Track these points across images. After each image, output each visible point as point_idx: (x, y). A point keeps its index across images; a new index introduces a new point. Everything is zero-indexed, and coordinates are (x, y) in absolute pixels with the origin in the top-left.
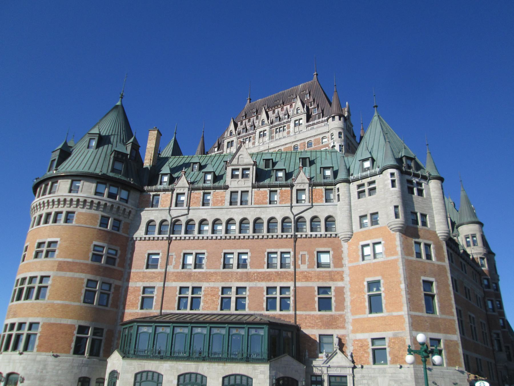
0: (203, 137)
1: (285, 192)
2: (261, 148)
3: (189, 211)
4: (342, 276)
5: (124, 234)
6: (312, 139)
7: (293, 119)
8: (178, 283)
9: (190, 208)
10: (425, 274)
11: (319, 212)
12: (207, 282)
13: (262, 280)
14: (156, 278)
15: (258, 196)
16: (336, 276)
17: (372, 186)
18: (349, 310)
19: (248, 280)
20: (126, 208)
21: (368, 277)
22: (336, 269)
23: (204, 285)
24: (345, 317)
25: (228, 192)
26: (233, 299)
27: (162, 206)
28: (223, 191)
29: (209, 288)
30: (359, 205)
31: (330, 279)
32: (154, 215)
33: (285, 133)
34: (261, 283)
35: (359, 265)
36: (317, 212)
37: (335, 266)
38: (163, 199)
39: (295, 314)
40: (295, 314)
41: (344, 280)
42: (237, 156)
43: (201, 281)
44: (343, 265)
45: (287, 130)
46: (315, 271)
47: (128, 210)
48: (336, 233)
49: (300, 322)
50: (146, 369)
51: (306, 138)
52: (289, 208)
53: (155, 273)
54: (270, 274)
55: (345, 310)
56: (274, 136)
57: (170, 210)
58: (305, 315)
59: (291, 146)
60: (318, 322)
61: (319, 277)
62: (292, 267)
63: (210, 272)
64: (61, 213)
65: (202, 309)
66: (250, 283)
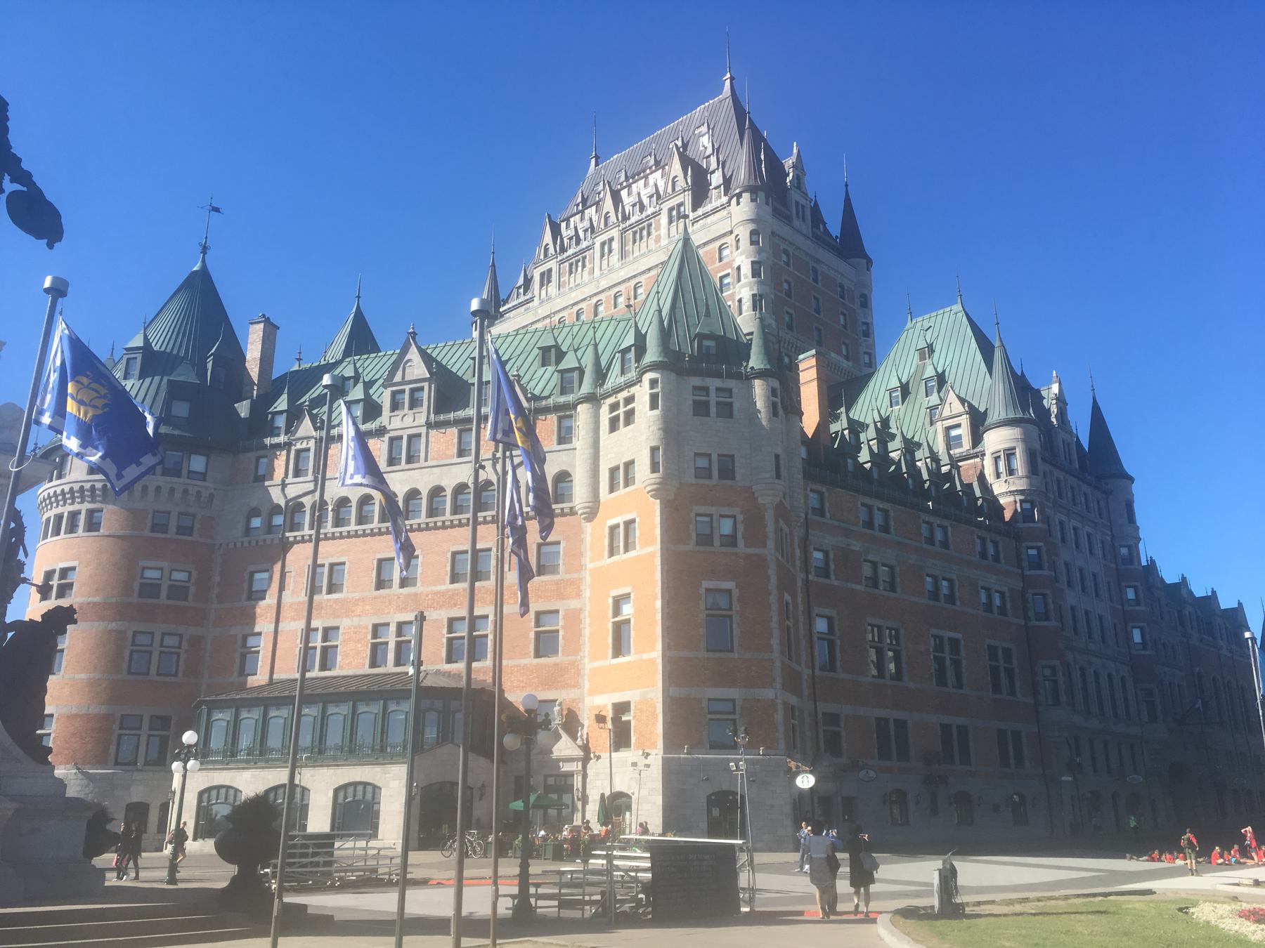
0: (493, 265)
2: (602, 284)
12: (347, 617)
13: (441, 607)
23: (345, 623)
25: (387, 437)
26: (392, 646)
34: (439, 612)
41: (581, 595)
43: (338, 617)
48: (570, 505)
50: (216, 783)
55: (581, 654)
58: (511, 667)
63: (353, 598)
64: (79, 512)
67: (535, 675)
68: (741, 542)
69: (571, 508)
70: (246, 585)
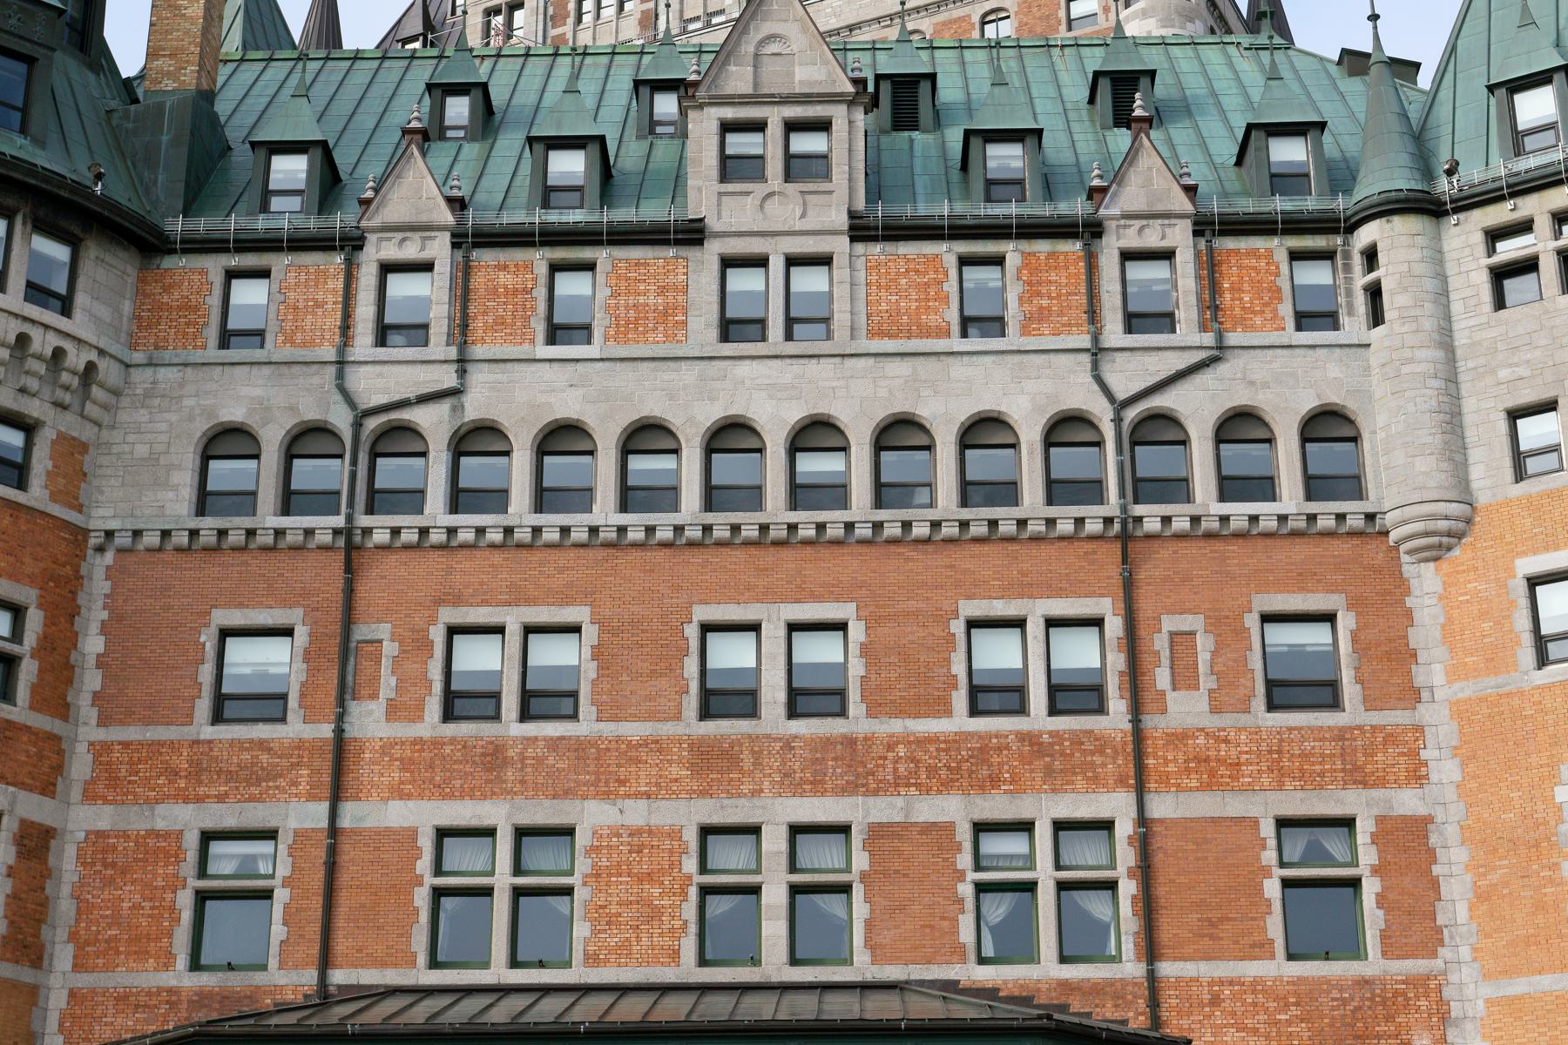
1: (1049, 269)
3: (462, 373)
4: (1414, 753)
5: (57, 510)
8: (424, 804)
9: (478, 351)
11: (1266, 386)
12: (606, 796)
13: (946, 786)
14: (281, 776)
15: (888, 288)
16: (1380, 757)
18: (1465, 952)
20: (68, 345)
22: (1376, 718)
24: (1446, 993)
27: (289, 340)
28: (671, 252)
29: (619, 835)
30: (1501, 346)
31: (1343, 770)
32: (245, 391)
35: (1521, 693)
36: (1252, 383)
37: (1370, 704)
38: (292, 295)
39: (1152, 977)
40: (1152, 977)
41: (1426, 777)
42: (748, 48)
43: (567, 794)
44: (1418, 691)
46: (1258, 731)
47: (77, 359)
49: (1185, 1023)
52: (1086, 359)
53: (269, 749)
54: (985, 748)
57: (341, 363)
58: (1211, 983)
60: (1289, 1023)
62: (1118, 706)
63: (618, 739)
65: (587, 956)
66: (871, 800)
67: (1294, 1011)
69: (1370, 517)
70: (206, 673)
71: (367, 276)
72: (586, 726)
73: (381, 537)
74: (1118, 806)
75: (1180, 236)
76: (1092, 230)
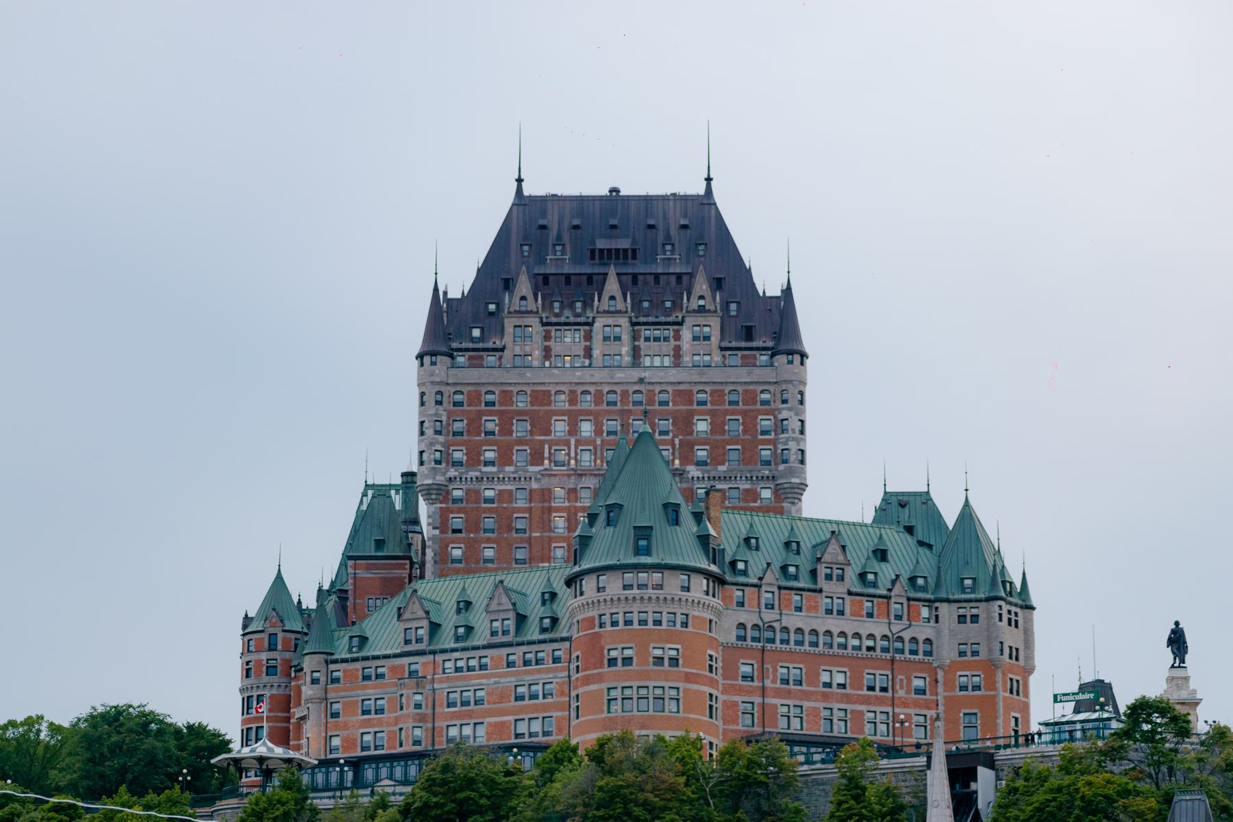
6: (740, 388)
7: (689, 321)
9: (783, 612)
10: (1013, 709)
12: (808, 701)
13: (862, 704)
17: (975, 611)
19: (848, 702)
21: (965, 708)
23: (806, 704)
33: (667, 347)
37: (931, 695)
39: (894, 741)
43: (801, 700)
45: (673, 343)
46: (912, 698)
51: (727, 383)
54: (869, 697)
56: (642, 346)
57: (760, 612)
59: (691, 391)
61: (916, 704)
62: (890, 691)
68: (1021, 694)
71: (763, 592)
72: (804, 687)
73: (769, 648)
74: (889, 709)
75: (904, 601)
76: (890, 597)
